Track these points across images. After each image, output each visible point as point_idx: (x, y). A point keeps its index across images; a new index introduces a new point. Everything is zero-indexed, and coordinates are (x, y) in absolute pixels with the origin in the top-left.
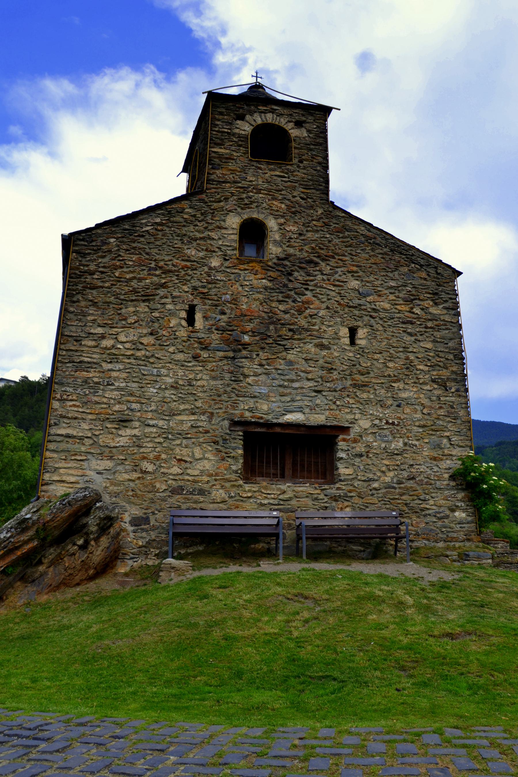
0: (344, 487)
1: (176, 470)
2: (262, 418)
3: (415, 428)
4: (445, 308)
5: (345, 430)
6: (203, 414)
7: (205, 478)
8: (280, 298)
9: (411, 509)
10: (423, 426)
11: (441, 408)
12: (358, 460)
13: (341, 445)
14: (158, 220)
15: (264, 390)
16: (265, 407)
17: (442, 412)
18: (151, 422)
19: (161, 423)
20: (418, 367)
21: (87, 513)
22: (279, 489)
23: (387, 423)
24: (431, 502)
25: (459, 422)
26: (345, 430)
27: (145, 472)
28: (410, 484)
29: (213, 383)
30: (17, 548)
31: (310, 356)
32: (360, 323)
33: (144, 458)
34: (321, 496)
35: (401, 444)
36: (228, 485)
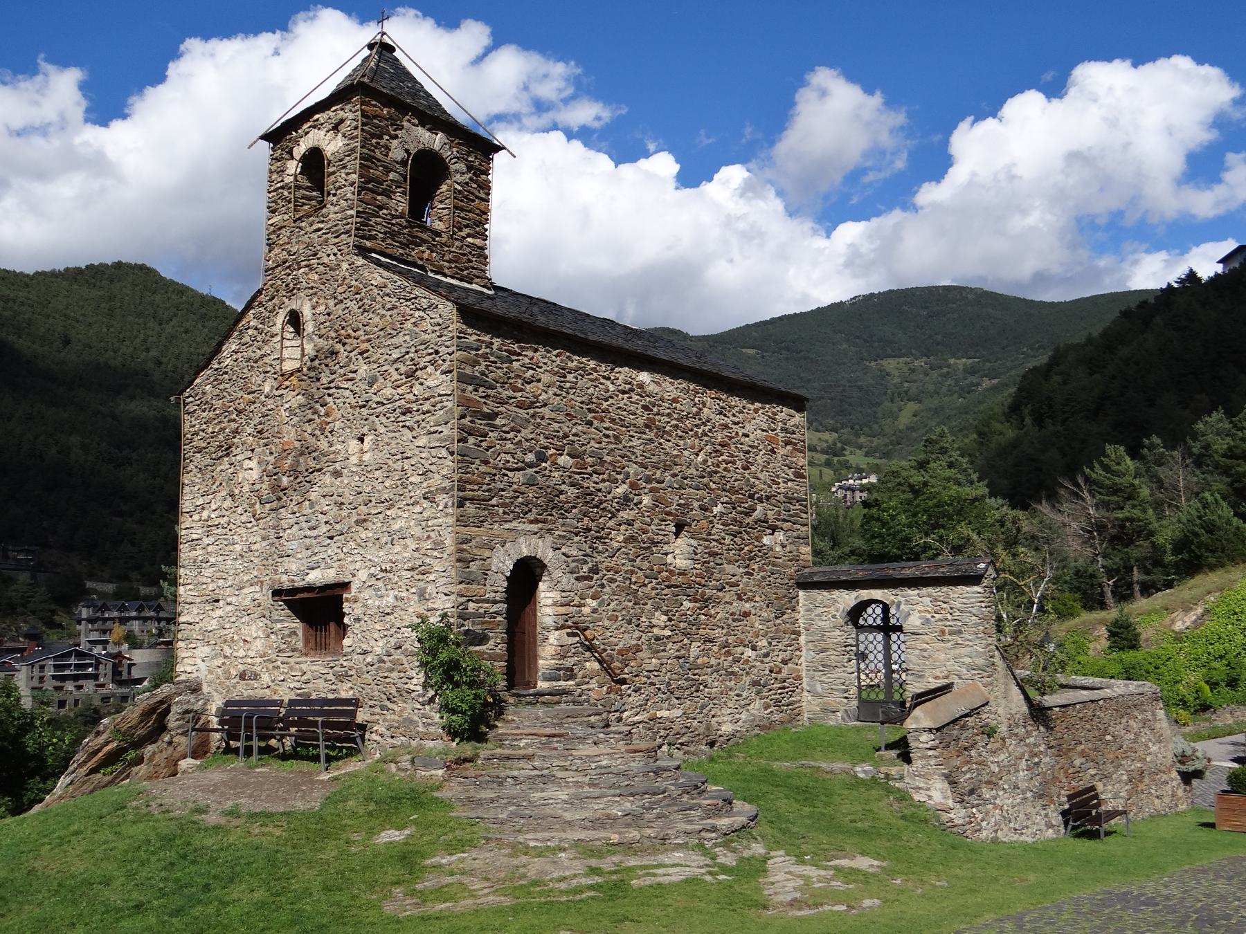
0: (345, 664)
1: (241, 653)
2: (293, 581)
3: (404, 573)
4: (444, 373)
5: (345, 586)
6: (257, 583)
7: (258, 660)
8: (310, 416)
9: (398, 690)
10: (412, 569)
11: (429, 537)
12: (357, 625)
13: (346, 607)
14: (234, 347)
15: (293, 545)
16: (294, 567)
17: (428, 544)
18: (229, 600)
19: (233, 599)
20: (412, 479)
21: (168, 711)
22: (301, 669)
23: (382, 571)
24: (415, 681)
25: (445, 556)
26: (345, 586)
27: (226, 657)
28: (397, 655)
29: (264, 544)
30: (99, 750)
31: (326, 490)
32: (365, 430)
33: (225, 641)
34: (330, 677)
35: (391, 600)
36: (270, 666)
